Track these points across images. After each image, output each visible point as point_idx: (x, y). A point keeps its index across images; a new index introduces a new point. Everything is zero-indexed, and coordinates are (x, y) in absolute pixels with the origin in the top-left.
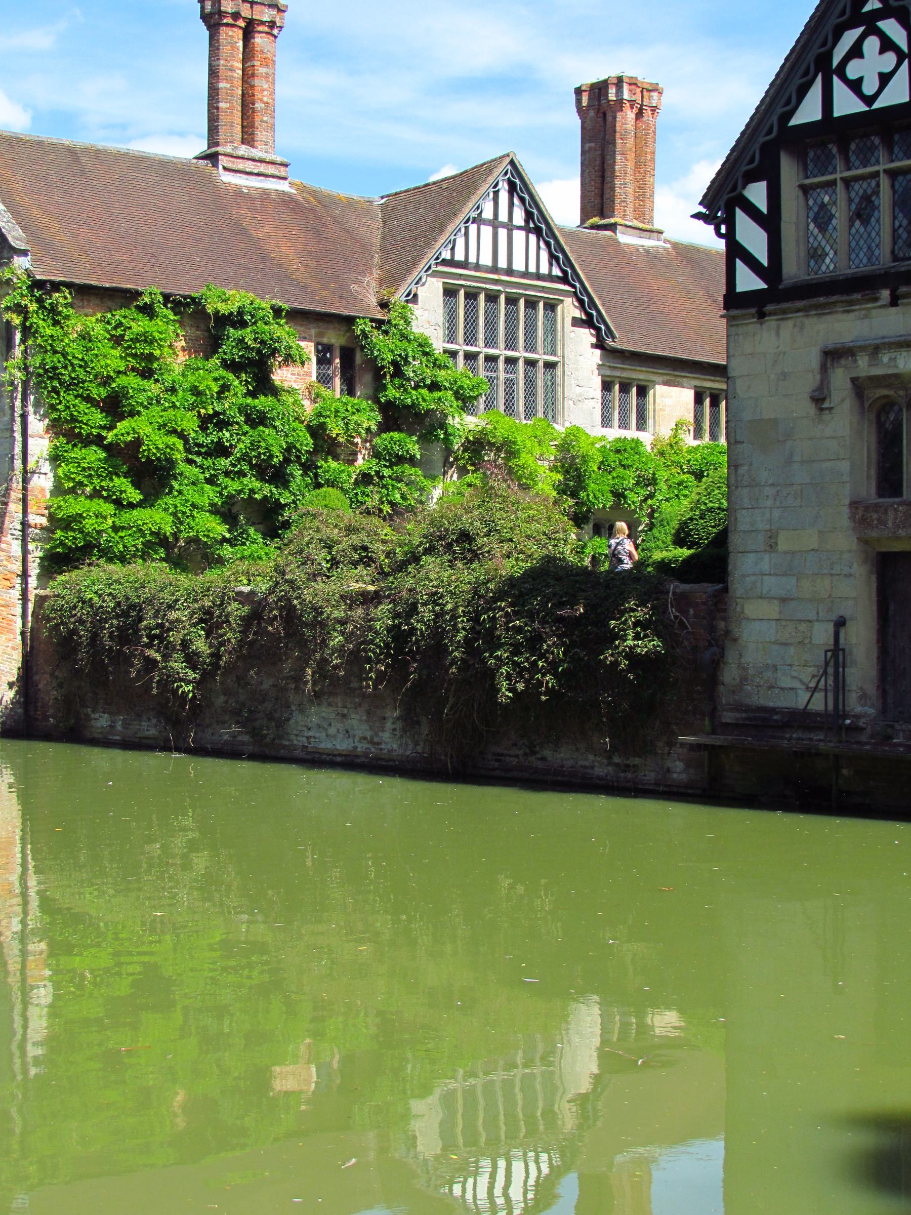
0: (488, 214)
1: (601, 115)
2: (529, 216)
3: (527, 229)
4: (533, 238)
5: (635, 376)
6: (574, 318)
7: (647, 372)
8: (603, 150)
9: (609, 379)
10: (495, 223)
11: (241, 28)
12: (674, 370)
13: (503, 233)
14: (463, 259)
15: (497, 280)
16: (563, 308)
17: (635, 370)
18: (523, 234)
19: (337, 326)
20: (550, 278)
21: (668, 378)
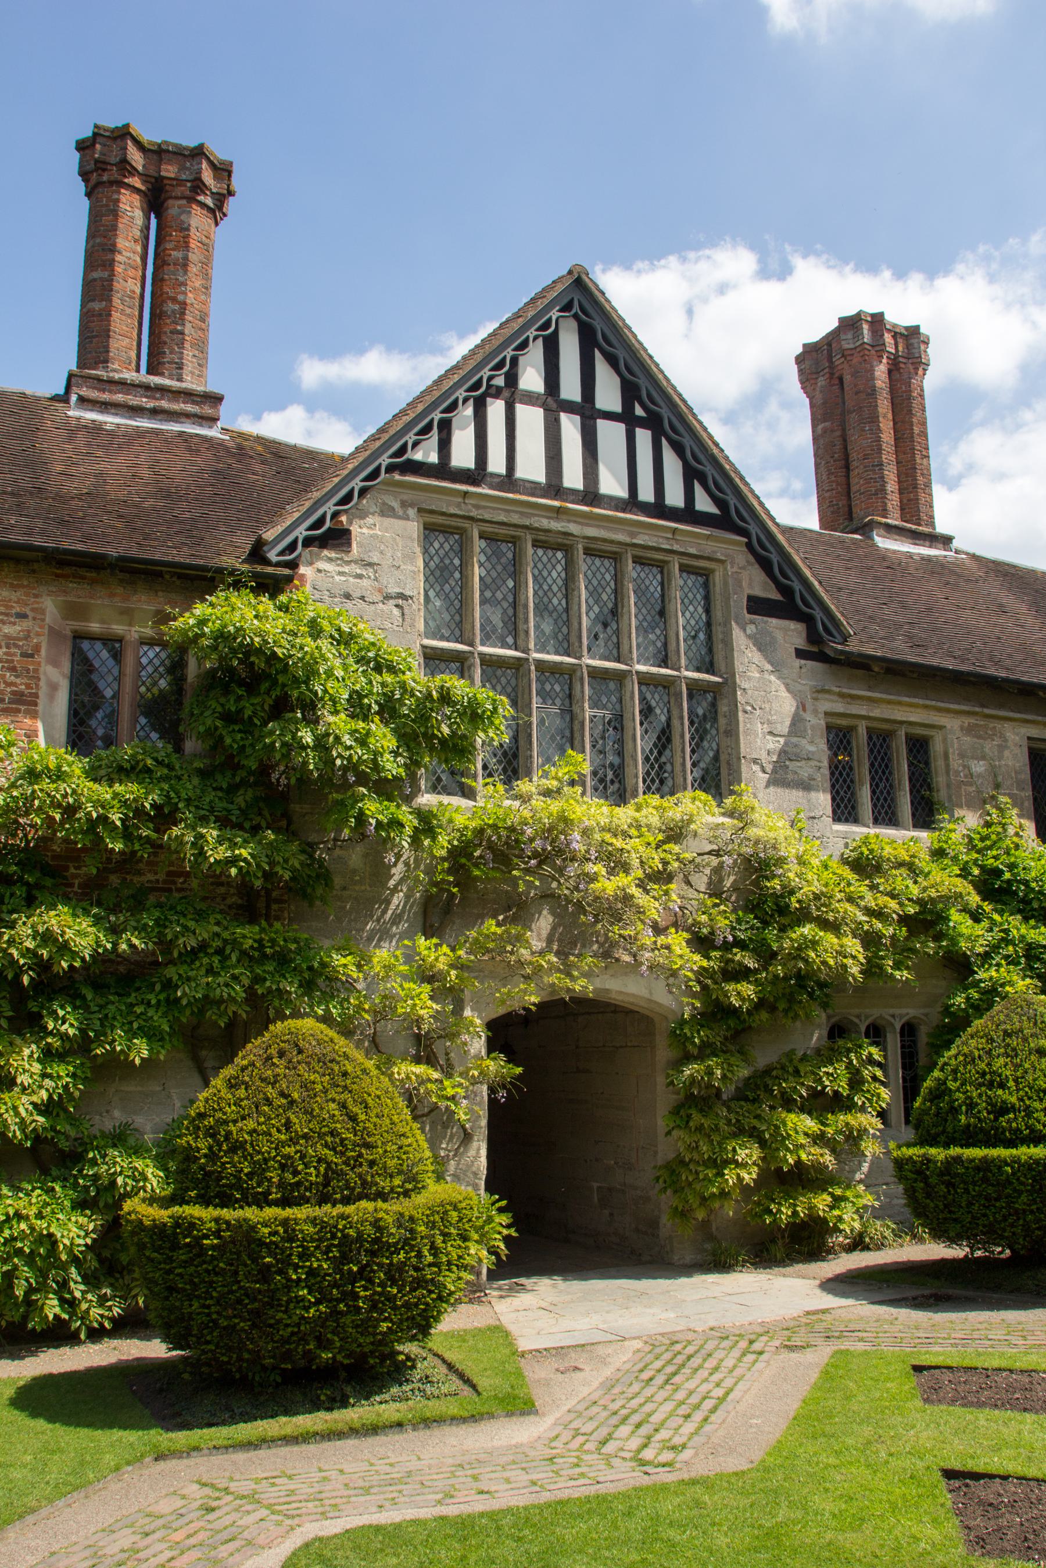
0: (531, 379)
1: (837, 382)
2: (630, 392)
3: (626, 417)
4: (644, 437)
5: (899, 714)
6: (751, 599)
7: (926, 707)
8: (844, 430)
9: (844, 722)
10: (552, 401)
11: (137, 191)
12: (983, 706)
13: (570, 427)
14: (471, 464)
15: (558, 510)
16: (725, 575)
17: (900, 703)
18: (620, 428)
19: (119, 590)
20: (688, 514)
21: (972, 720)
